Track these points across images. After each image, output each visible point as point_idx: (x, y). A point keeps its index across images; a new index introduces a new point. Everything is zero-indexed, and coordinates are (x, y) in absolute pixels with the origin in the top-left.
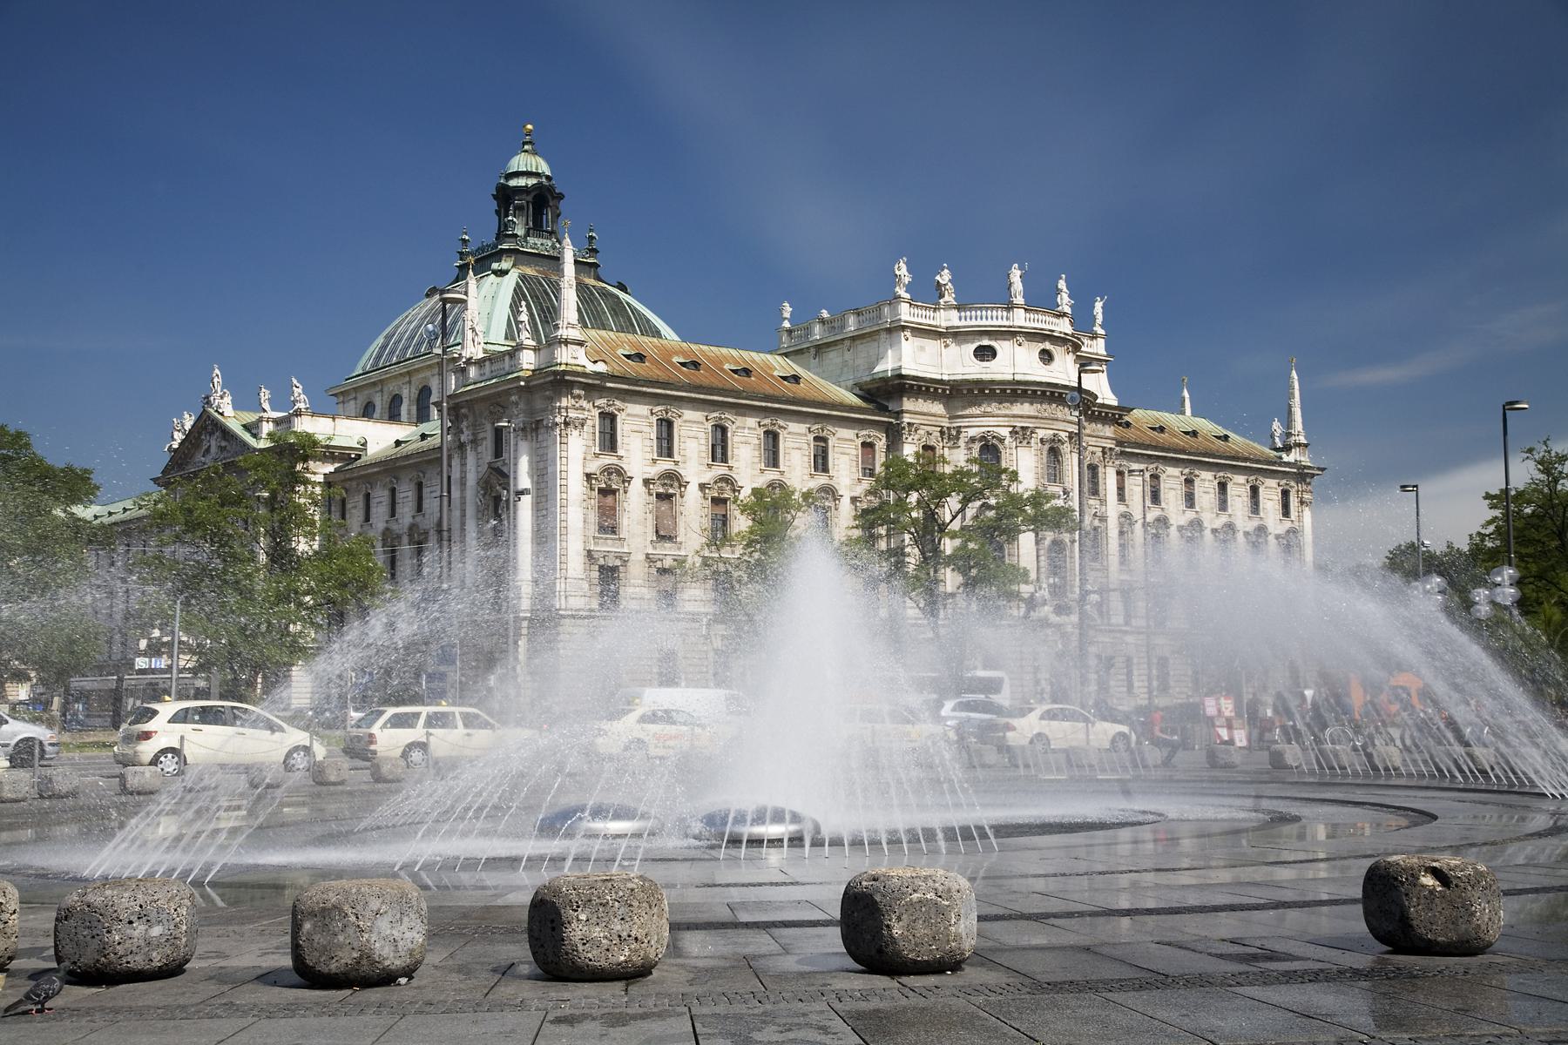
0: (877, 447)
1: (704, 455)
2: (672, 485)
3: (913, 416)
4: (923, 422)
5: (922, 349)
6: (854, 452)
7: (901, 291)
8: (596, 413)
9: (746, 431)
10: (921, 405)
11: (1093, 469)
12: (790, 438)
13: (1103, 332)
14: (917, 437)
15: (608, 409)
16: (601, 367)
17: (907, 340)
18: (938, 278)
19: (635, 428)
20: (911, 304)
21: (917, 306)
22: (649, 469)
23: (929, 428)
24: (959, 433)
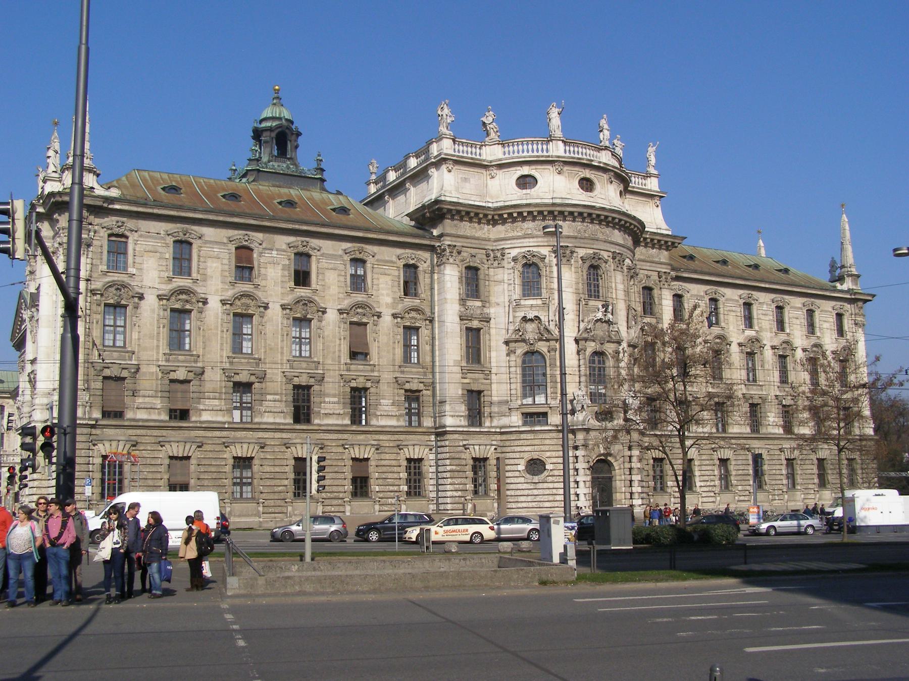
0: (420, 269)
1: (227, 274)
2: (187, 301)
3: (454, 239)
4: (465, 245)
5: (466, 180)
6: (396, 273)
7: (443, 129)
8: (104, 234)
9: (274, 252)
10: (466, 228)
11: (648, 290)
12: (324, 263)
13: (656, 172)
14: (460, 257)
15: (116, 230)
16: (114, 193)
17: (450, 171)
18: (484, 119)
19: (149, 248)
20: (454, 141)
21: (463, 143)
22: (163, 287)
23: (473, 251)
24: (503, 255)
